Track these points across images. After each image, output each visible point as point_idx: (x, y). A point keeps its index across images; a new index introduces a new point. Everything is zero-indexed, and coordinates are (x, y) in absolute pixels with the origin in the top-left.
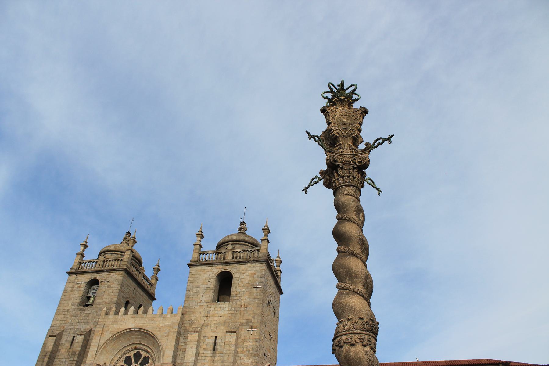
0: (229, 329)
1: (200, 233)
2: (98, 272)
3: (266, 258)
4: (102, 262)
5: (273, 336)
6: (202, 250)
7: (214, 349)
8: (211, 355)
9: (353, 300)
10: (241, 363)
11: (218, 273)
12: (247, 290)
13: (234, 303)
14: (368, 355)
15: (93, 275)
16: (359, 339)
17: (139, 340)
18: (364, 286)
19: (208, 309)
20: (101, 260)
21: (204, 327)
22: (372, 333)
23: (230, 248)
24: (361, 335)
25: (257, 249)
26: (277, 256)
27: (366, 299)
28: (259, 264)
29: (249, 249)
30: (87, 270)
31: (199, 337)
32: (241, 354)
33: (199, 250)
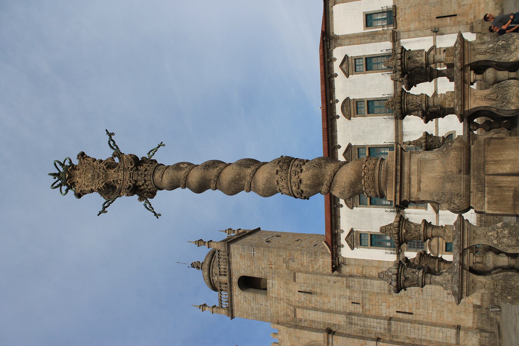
0: (292, 279)
1: (201, 307)
3: (226, 244)
5: (298, 238)
6: (217, 305)
7: (310, 293)
8: (316, 295)
9: (261, 179)
11: (240, 290)
12: (256, 262)
13: (267, 274)
14: (310, 168)
16: (295, 175)
18: (248, 167)
19: (274, 299)
21: (290, 303)
22: (290, 163)
23: (216, 278)
24: (292, 173)
25: (217, 252)
26: (224, 233)
27: (260, 166)
28: (232, 250)
29: (217, 259)
31: (299, 307)
32: (314, 268)
33: (218, 308)
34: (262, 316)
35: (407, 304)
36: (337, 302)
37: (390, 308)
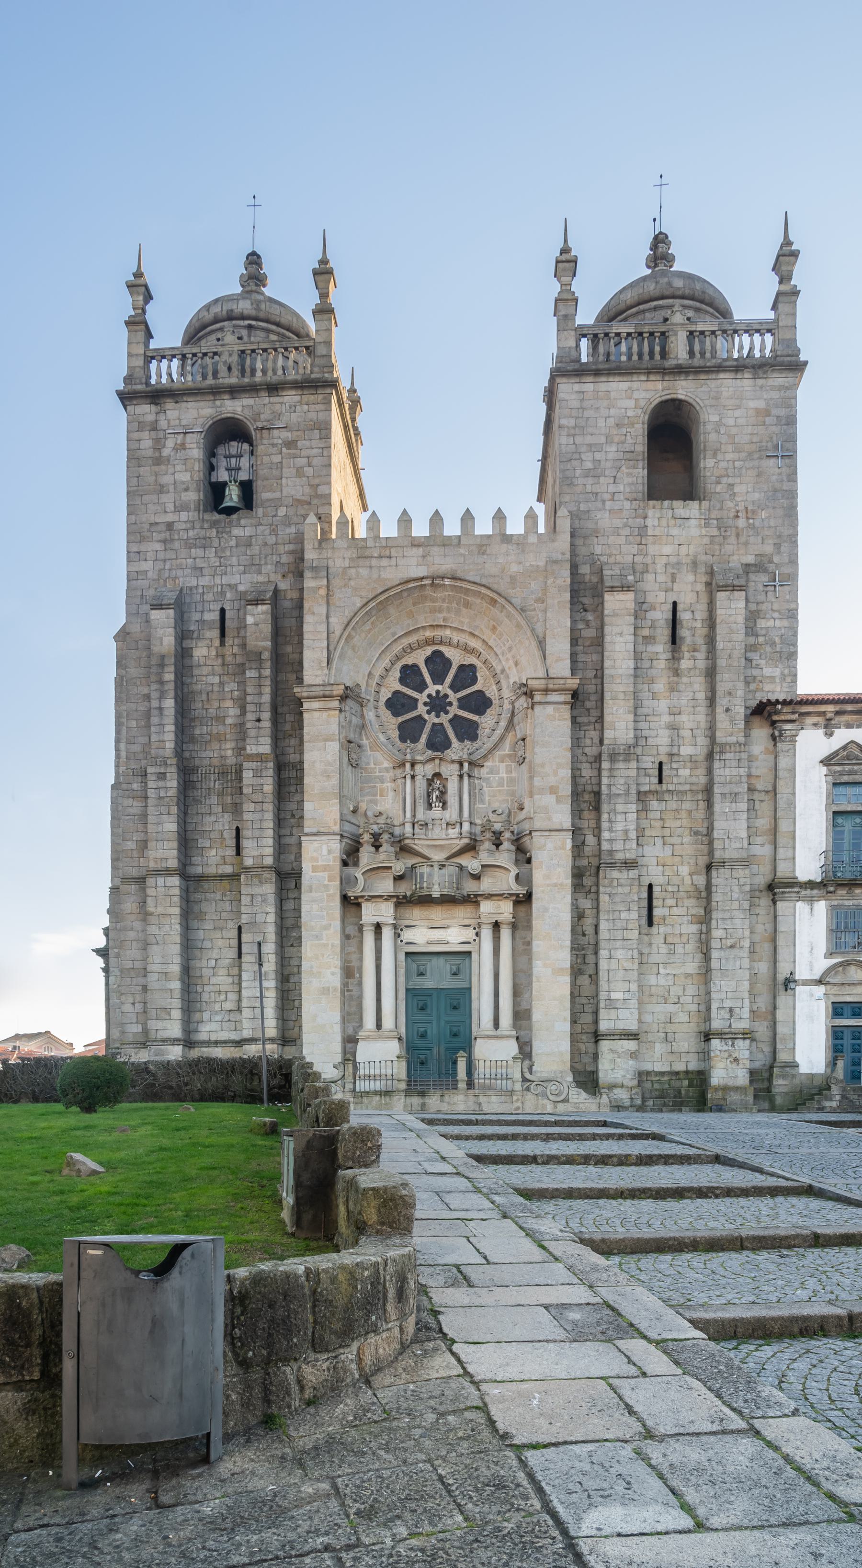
2: (234, 391)
4: (235, 358)
7: (674, 639)
8: (669, 655)
10: (755, 677)
12: (748, 464)
15: (218, 403)
17: (441, 616)
20: (228, 348)
30: (190, 384)
34: (576, 482)
35: (675, 911)
36: (656, 718)
37: (661, 868)
